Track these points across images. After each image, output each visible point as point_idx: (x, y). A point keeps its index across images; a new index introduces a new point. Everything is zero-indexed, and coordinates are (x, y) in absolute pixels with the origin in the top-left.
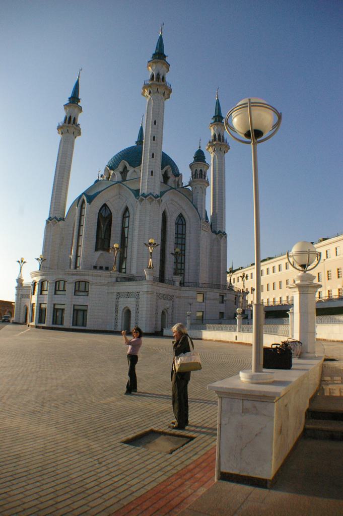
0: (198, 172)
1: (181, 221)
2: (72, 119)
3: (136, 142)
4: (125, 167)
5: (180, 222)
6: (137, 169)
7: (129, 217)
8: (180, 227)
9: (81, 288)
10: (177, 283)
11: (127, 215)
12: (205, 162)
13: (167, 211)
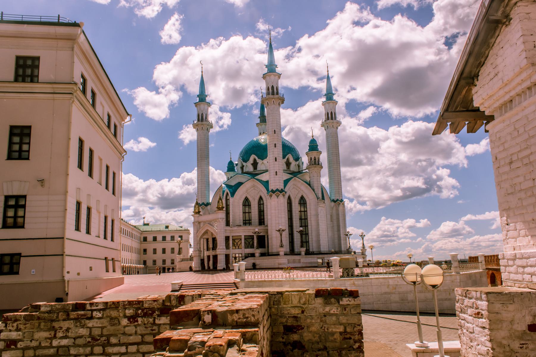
0: (313, 160)
1: (303, 202)
2: (204, 118)
4: (255, 160)
5: (302, 202)
6: (265, 161)
7: (263, 204)
10: (303, 253)
11: (262, 203)
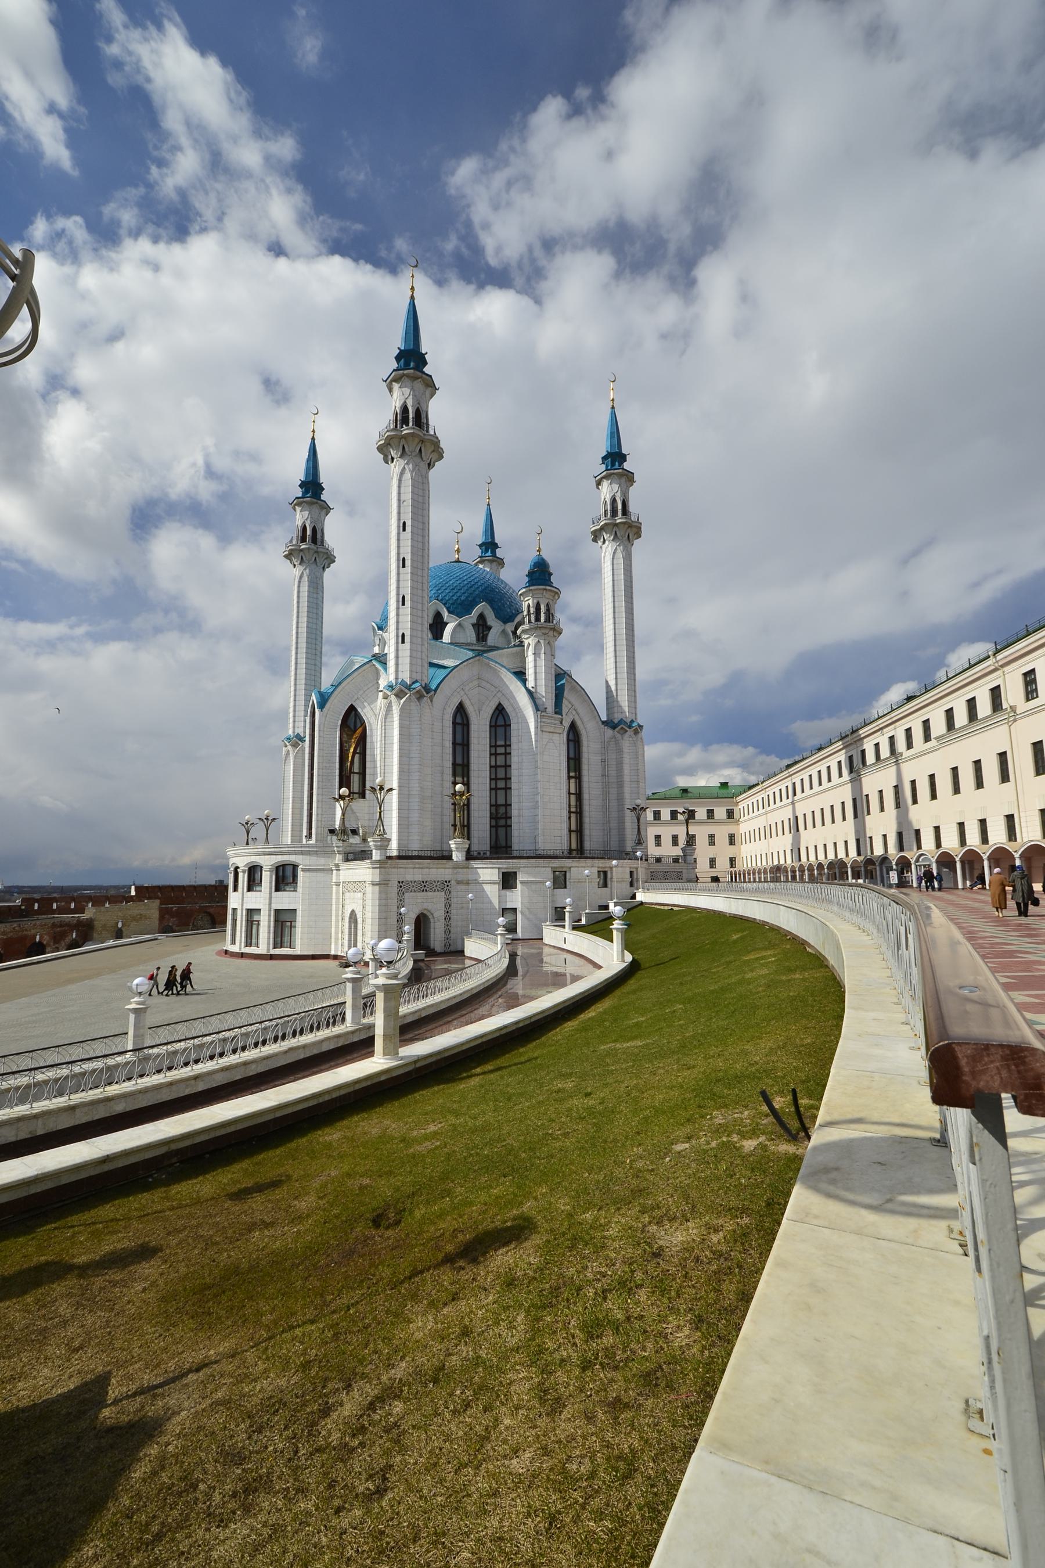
1: (501, 720)
2: (309, 532)
3: (480, 546)
5: (501, 722)
8: (501, 731)
9: (285, 876)
10: (457, 856)
12: (550, 584)
13: (468, 705)
